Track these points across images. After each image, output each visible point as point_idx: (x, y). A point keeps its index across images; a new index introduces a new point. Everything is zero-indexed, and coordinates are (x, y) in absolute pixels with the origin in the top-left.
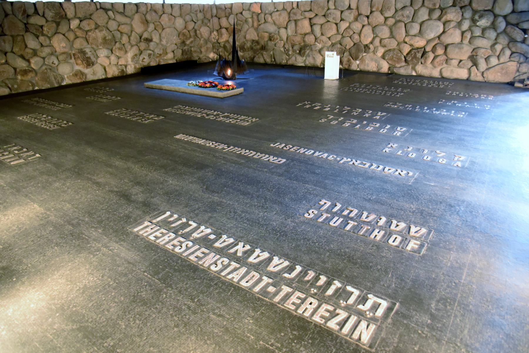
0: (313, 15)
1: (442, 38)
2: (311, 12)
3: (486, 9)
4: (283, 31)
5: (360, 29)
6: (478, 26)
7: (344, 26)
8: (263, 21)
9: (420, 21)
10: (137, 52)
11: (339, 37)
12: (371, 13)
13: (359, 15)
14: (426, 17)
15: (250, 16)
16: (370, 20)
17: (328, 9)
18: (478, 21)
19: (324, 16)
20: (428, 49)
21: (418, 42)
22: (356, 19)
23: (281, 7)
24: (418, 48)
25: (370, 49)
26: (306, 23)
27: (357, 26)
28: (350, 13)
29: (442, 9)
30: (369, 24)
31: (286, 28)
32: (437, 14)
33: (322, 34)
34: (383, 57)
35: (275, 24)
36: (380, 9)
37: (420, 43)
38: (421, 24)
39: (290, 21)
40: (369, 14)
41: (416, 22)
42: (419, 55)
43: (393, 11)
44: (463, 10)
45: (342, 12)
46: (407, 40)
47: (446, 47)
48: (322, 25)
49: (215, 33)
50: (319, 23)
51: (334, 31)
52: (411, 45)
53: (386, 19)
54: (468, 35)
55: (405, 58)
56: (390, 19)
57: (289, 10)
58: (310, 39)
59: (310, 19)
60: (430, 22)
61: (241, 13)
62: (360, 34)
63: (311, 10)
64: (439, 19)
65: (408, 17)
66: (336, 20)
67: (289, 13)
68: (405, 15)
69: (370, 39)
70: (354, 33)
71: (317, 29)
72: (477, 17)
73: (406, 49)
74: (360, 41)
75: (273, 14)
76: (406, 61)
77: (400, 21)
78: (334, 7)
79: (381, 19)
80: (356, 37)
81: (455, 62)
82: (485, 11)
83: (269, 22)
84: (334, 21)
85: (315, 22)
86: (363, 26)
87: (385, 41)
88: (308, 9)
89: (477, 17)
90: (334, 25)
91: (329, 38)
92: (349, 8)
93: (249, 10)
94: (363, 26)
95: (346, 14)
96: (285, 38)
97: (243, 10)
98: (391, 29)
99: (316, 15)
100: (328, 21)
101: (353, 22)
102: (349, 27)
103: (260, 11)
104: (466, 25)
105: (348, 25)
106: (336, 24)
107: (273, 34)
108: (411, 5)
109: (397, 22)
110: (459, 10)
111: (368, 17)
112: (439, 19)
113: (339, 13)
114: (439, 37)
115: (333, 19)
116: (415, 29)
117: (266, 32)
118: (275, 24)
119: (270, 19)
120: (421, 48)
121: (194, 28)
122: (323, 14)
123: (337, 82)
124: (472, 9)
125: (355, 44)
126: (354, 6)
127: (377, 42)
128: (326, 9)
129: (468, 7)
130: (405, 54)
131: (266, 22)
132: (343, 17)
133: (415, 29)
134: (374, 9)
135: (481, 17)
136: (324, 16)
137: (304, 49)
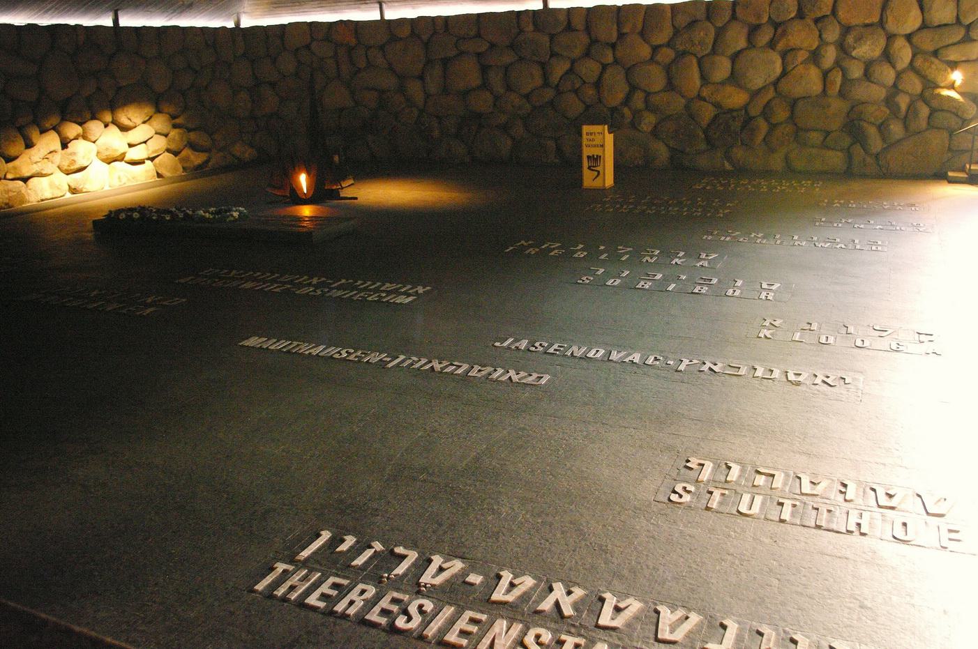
0: (484, 47)
1: (784, 86)
3: (867, 22)
4: (414, 88)
5: (597, 73)
6: (854, 58)
7: (560, 68)
8: (363, 64)
9: (730, 52)
10: (58, 145)
11: (549, 94)
13: (594, 41)
14: (742, 43)
15: (332, 54)
16: (619, 54)
18: (854, 48)
20: (755, 111)
21: (729, 97)
22: (587, 54)
23: (406, 31)
24: (731, 111)
25: (623, 116)
27: (590, 69)
29: (776, 25)
31: (421, 78)
32: (765, 37)
33: (509, 88)
34: (655, 133)
35: (391, 68)
37: (736, 98)
38: (735, 58)
39: (429, 62)
41: (723, 54)
42: (736, 126)
44: (820, 25)
46: (705, 93)
47: (793, 104)
48: (507, 69)
49: (244, 95)
51: (539, 81)
52: (717, 105)
53: (655, 49)
54: (837, 78)
55: (705, 132)
56: (664, 49)
57: (425, 37)
60: (753, 53)
61: (308, 47)
62: (598, 84)
63: (478, 35)
64: (772, 45)
65: (701, 43)
67: (427, 45)
69: (621, 96)
70: (584, 82)
71: (496, 79)
73: (707, 113)
74: (600, 101)
76: (708, 140)
77: (684, 54)
78: (531, 28)
79: (645, 51)
80: (590, 92)
81: (815, 137)
82: (867, 26)
86: (604, 67)
87: (656, 100)
88: (472, 33)
89: (850, 39)
91: (527, 97)
93: (327, 39)
94: (604, 67)
96: (419, 98)
97: (313, 39)
98: (668, 69)
99: (492, 46)
100: (521, 59)
103: (353, 42)
104: (830, 55)
105: (567, 66)
106: (543, 65)
108: (708, 18)
109: (682, 54)
110: (813, 26)
111: (613, 46)
112: (772, 45)
113: (546, 39)
114: (775, 84)
116: (722, 68)
117: (373, 89)
118: (393, 71)
119: (380, 60)
120: (741, 110)
121: (192, 86)
124: (839, 23)
125: (588, 107)
127: (638, 101)
128: (515, 31)
130: (704, 123)
131: (370, 65)
132: (556, 49)
133: (722, 68)
134: (625, 30)
135: (859, 39)
136: (512, 46)
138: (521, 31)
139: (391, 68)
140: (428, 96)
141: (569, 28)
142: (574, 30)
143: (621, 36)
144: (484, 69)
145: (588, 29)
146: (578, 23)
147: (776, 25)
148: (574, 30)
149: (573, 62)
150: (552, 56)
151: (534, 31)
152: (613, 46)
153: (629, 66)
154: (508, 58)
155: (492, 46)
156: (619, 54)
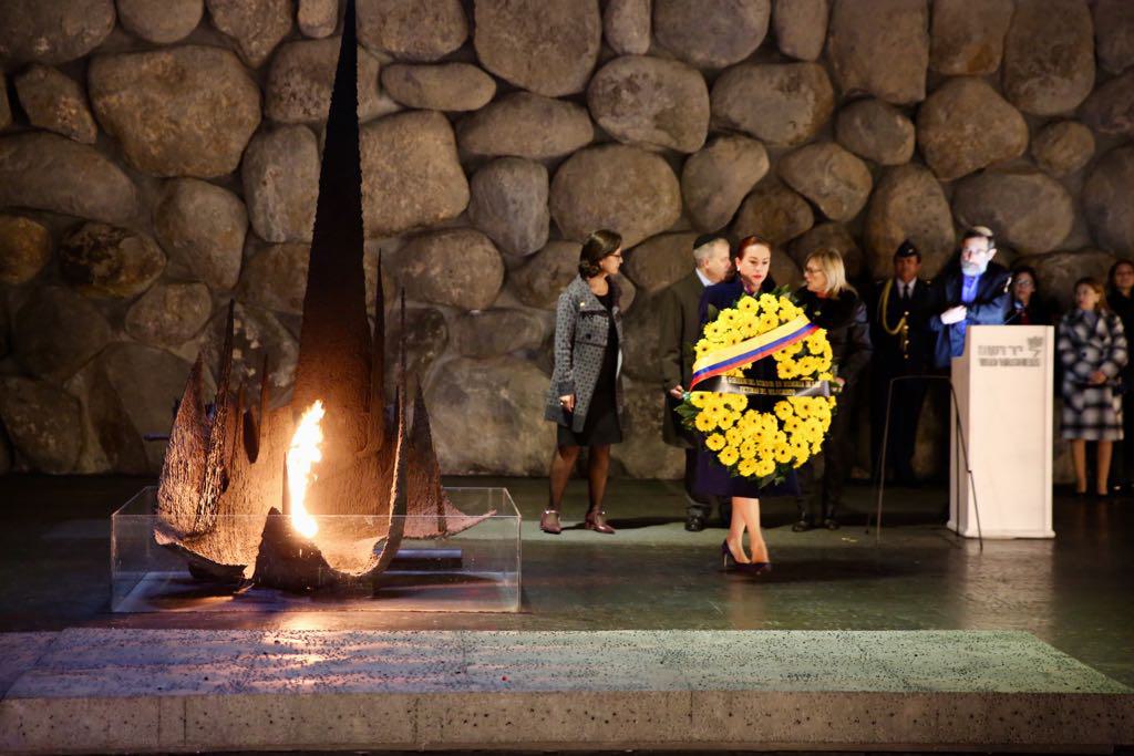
0: (484, 94)
2: (471, 70)
4: (210, 213)
7: (743, 169)
12: (929, 92)
19: (581, 100)
26: (434, 148)
28: (792, 87)
30: (920, 156)
31: (238, 183)
36: (993, 69)
40: (922, 97)
43: (1084, 78)
45: (714, 78)
48: (554, 166)
50: (537, 149)
57: (259, 49)
58: (469, 271)
59: (460, 122)
66: (677, 133)
75: (98, 73)
79: (1012, 130)
83: (65, 136)
84: (663, 137)
85: (508, 145)
88: (447, 47)
90: (665, 169)
92: (771, 50)
94: (882, 176)
95: (757, 96)
96: (228, 254)
99: (507, 92)
100: (603, 140)
101: (798, 146)
102: (777, 182)
105: (764, 165)
106: (679, 161)
107: (102, 233)
111: (914, 112)
113: (697, 84)
115: (660, 121)
122: (572, 83)
123: (1049, 546)
126: (804, 36)
128: (593, 48)
134: (958, 66)
136: (581, 100)
137: (419, 348)
138: (609, 53)
139: (112, 141)
140: (256, 243)
142: (791, 60)
143: (937, 82)
144: (474, 167)
145: (824, 57)
149: (779, 159)
150: (712, 138)
151: (649, 54)
152: (914, 112)
153: (961, 172)
154: (569, 133)
155: (507, 92)
156: (935, 138)
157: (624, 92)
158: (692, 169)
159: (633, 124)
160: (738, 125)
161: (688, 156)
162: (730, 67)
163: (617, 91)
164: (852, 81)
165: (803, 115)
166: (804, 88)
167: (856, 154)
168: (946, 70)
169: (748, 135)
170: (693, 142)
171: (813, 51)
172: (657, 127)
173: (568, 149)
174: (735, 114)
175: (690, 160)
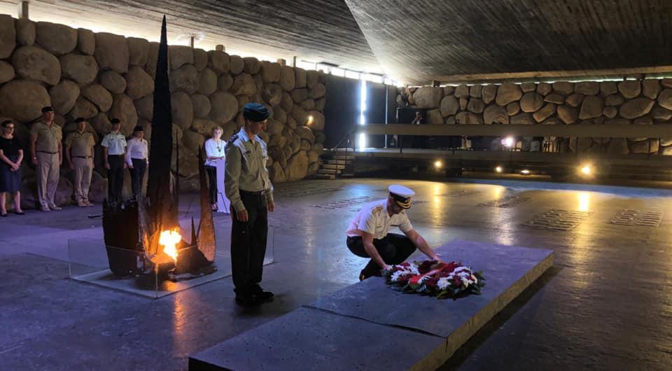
17: (20, 44)
18: (271, 97)
46: (198, 125)
64: (232, 91)
68: (191, 81)
70: (100, 111)
72: (268, 91)
82: (274, 83)
84: (45, 79)
100: (18, 77)
102: (83, 97)
106: (49, 87)
115: (43, 71)
129: (259, 76)
134: (137, 63)
135: (273, 91)
136: (10, 60)
138: (20, 44)
141: (78, 50)
142: (85, 54)
143: (130, 67)
146: (89, 47)
147: (234, 76)
148: (85, 54)
150: (61, 80)
157: (30, 61)
158: (54, 91)
159: (34, 72)
160: (70, 76)
161: (53, 86)
162: (65, 54)
163: (27, 59)
164: (106, 64)
165: (93, 72)
166: (92, 64)
167: (108, 90)
168: (133, 63)
169: (72, 80)
170: (55, 81)
171: (92, 53)
172: (44, 75)
173: (7, 80)
174: (70, 72)
175: (53, 88)
